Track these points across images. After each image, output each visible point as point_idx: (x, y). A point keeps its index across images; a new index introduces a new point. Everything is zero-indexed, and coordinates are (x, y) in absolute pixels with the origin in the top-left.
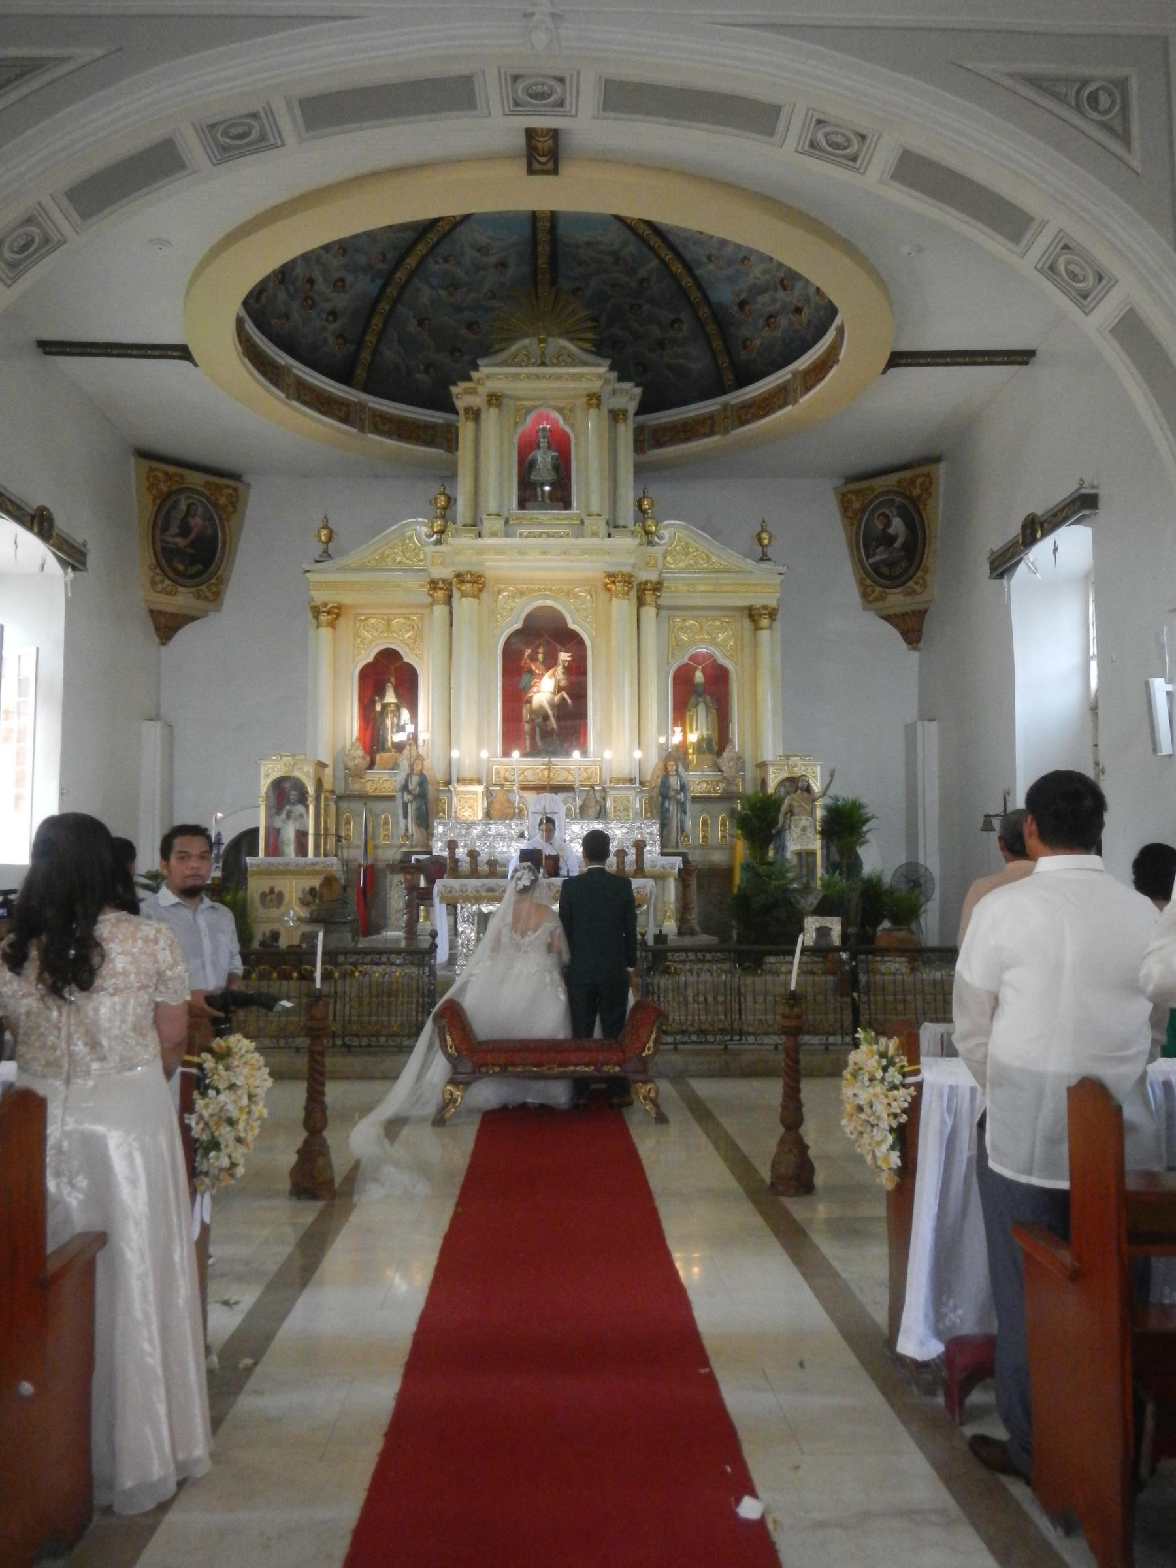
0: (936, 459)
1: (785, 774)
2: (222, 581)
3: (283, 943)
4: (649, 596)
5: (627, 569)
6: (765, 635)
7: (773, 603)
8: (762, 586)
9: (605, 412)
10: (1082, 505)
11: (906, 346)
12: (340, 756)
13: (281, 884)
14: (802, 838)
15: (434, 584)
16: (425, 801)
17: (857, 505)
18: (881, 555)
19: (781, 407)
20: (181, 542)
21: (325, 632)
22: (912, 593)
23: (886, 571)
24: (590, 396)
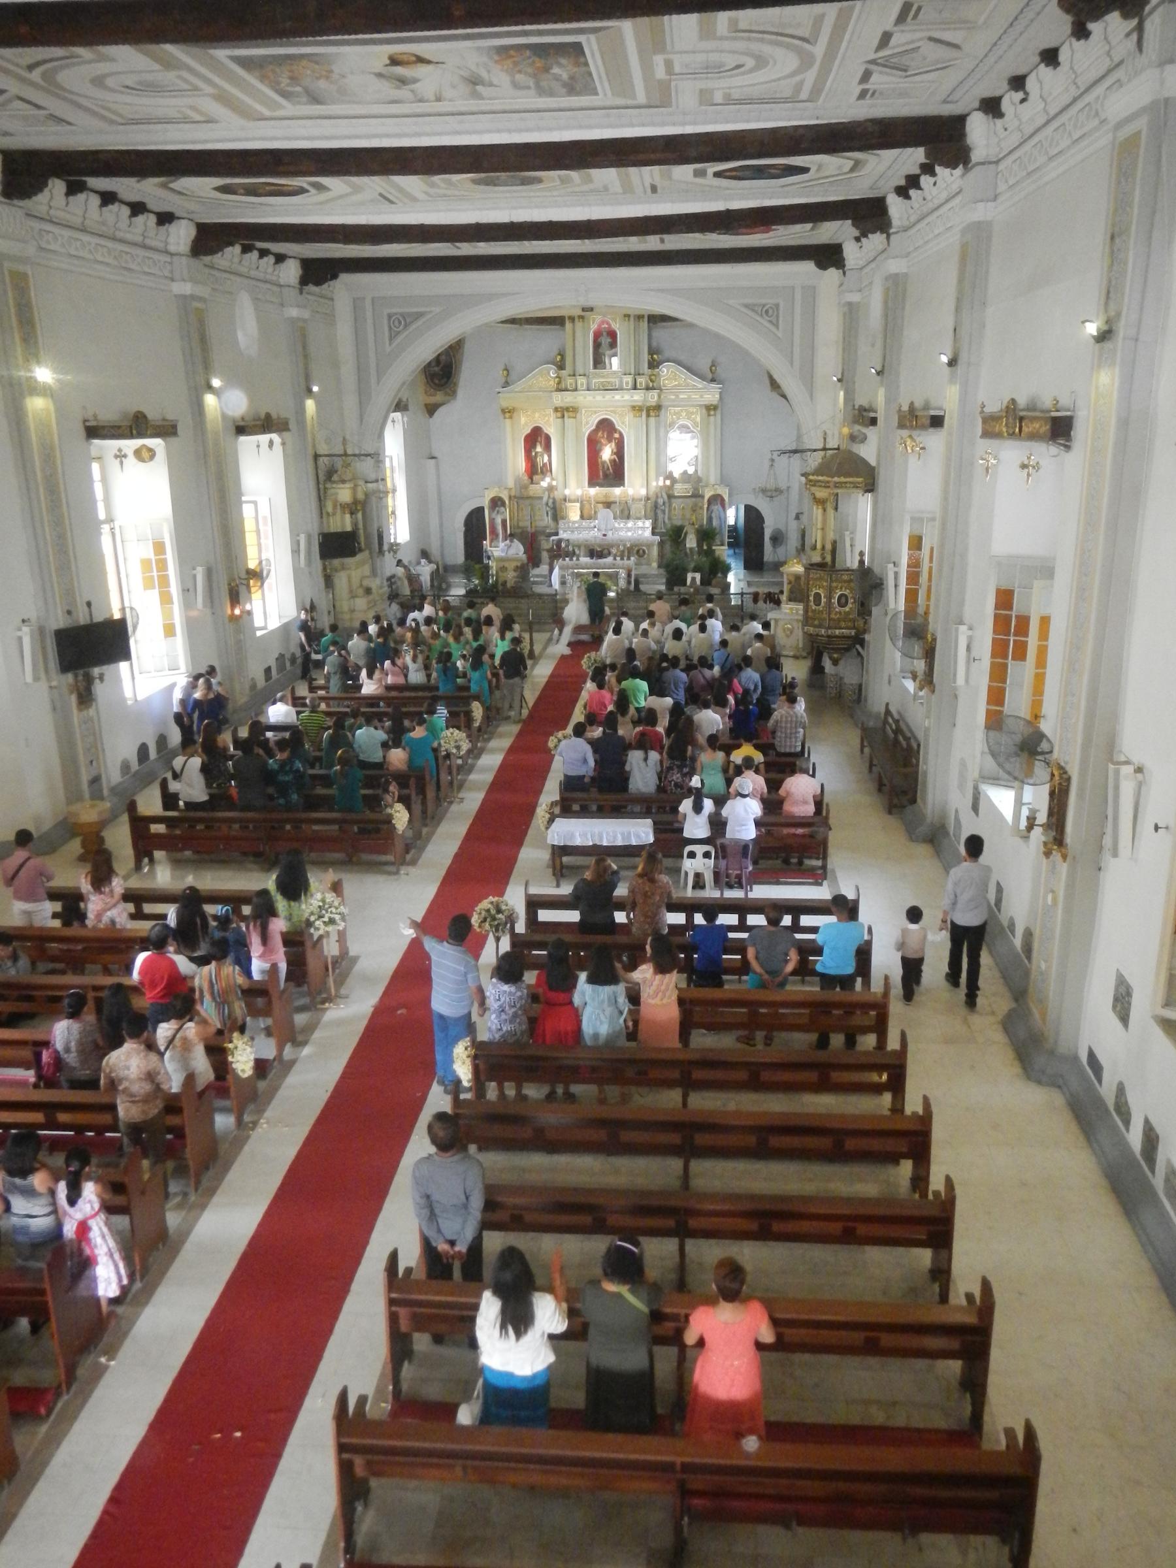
1: (712, 493)
2: (455, 385)
3: (509, 585)
4: (652, 413)
6: (712, 418)
7: (715, 403)
8: (711, 394)
12: (518, 480)
13: (506, 565)
14: (691, 542)
15: (556, 410)
16: (557, 512)
20: (436, 369)
21: (508, 421)
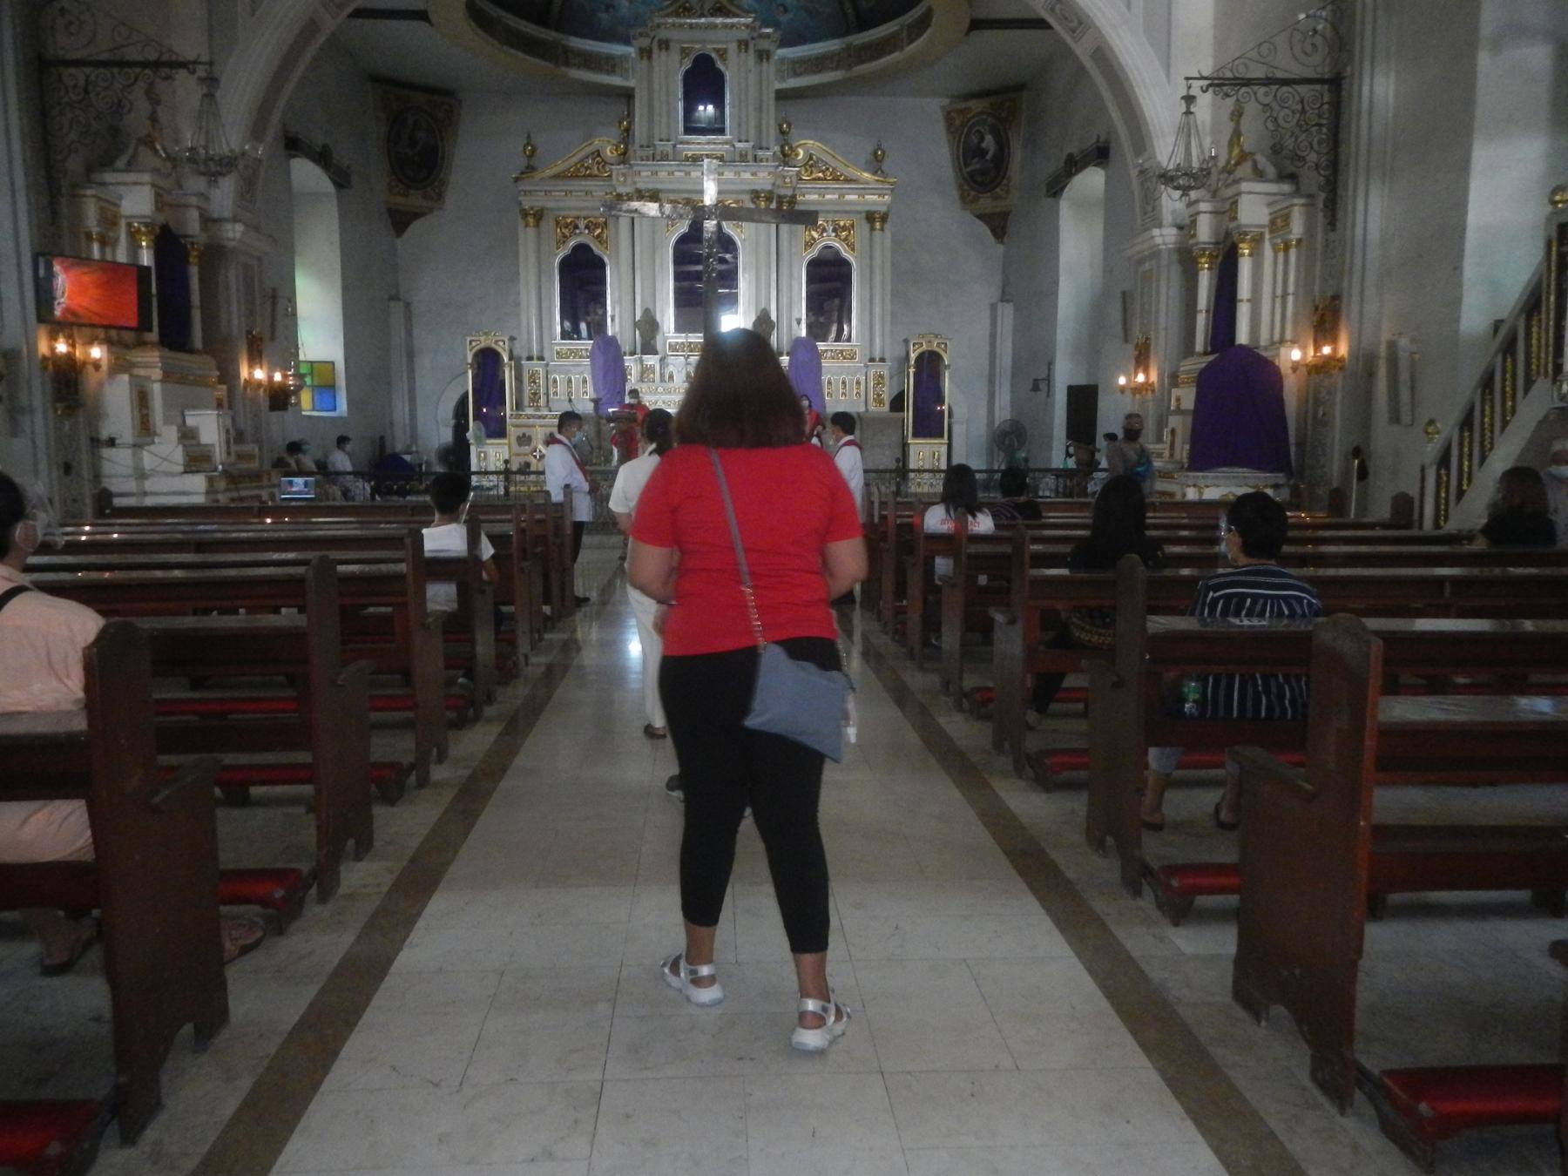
0: (1020, 87)
2: (443, 183)
5: (769, 187)
6: (877, 233)
7: (884, 209)
9: (751, 51)
10: (1101, 154)
11: (982, 14)
17: (958, 122)
18: (976, 165)
19: (892, 52)
21: (531, 231)
22: (997, 198)
23: (979, 179)
24: (740, 42)
